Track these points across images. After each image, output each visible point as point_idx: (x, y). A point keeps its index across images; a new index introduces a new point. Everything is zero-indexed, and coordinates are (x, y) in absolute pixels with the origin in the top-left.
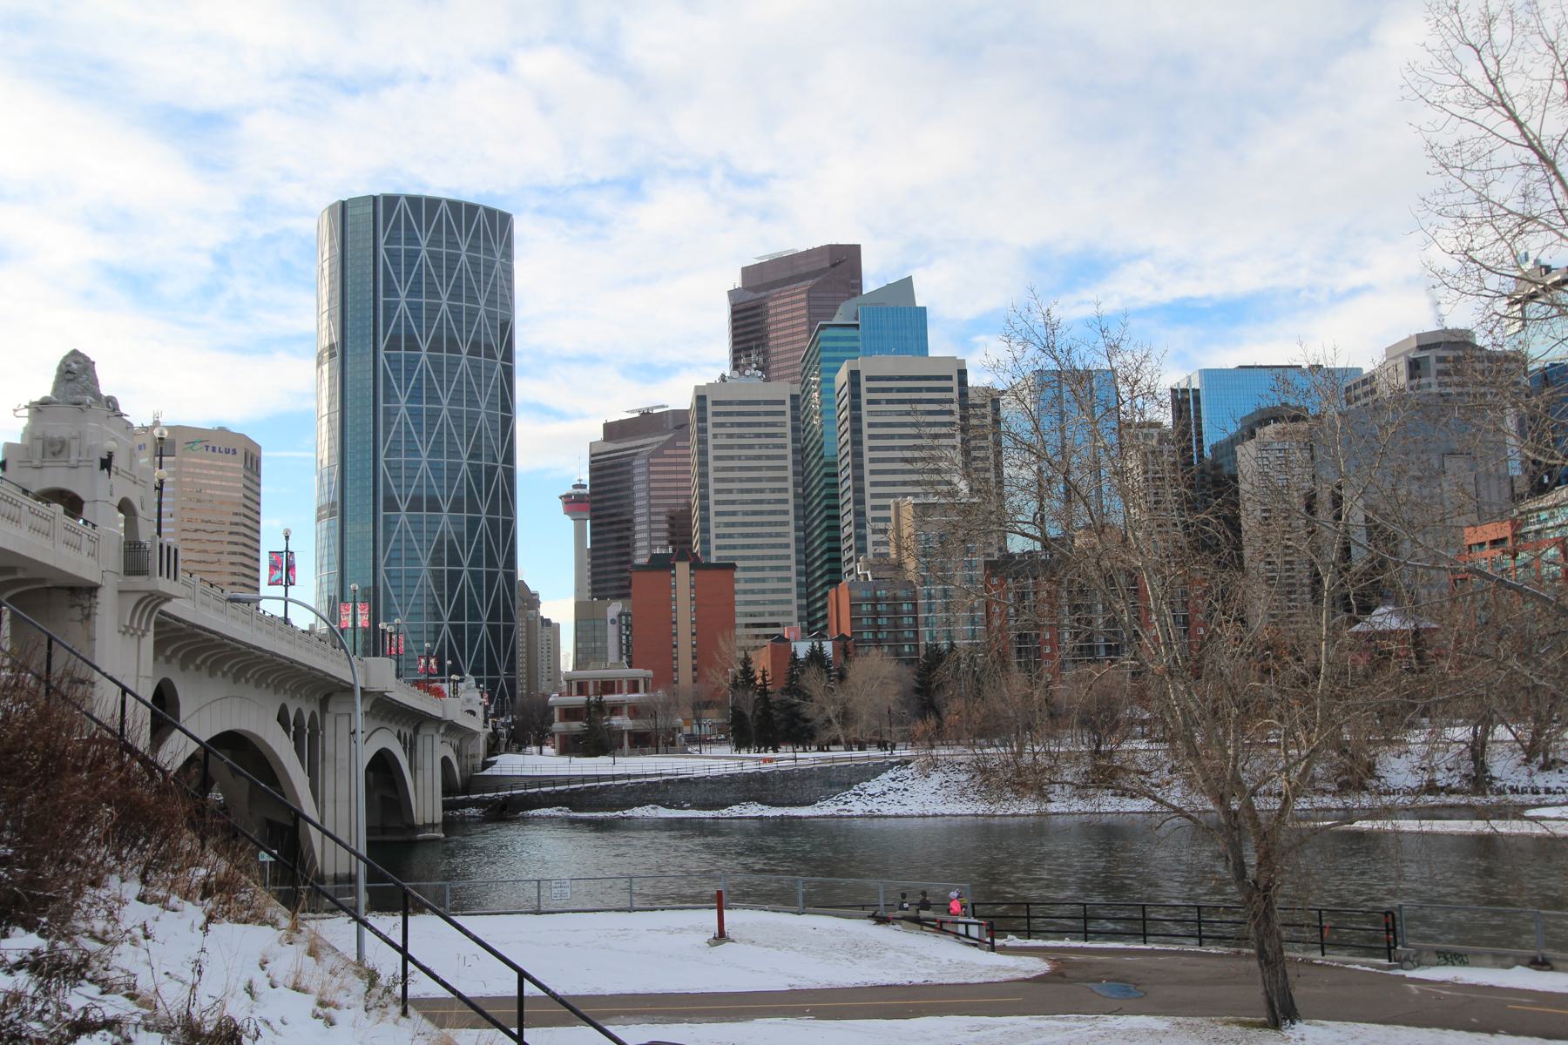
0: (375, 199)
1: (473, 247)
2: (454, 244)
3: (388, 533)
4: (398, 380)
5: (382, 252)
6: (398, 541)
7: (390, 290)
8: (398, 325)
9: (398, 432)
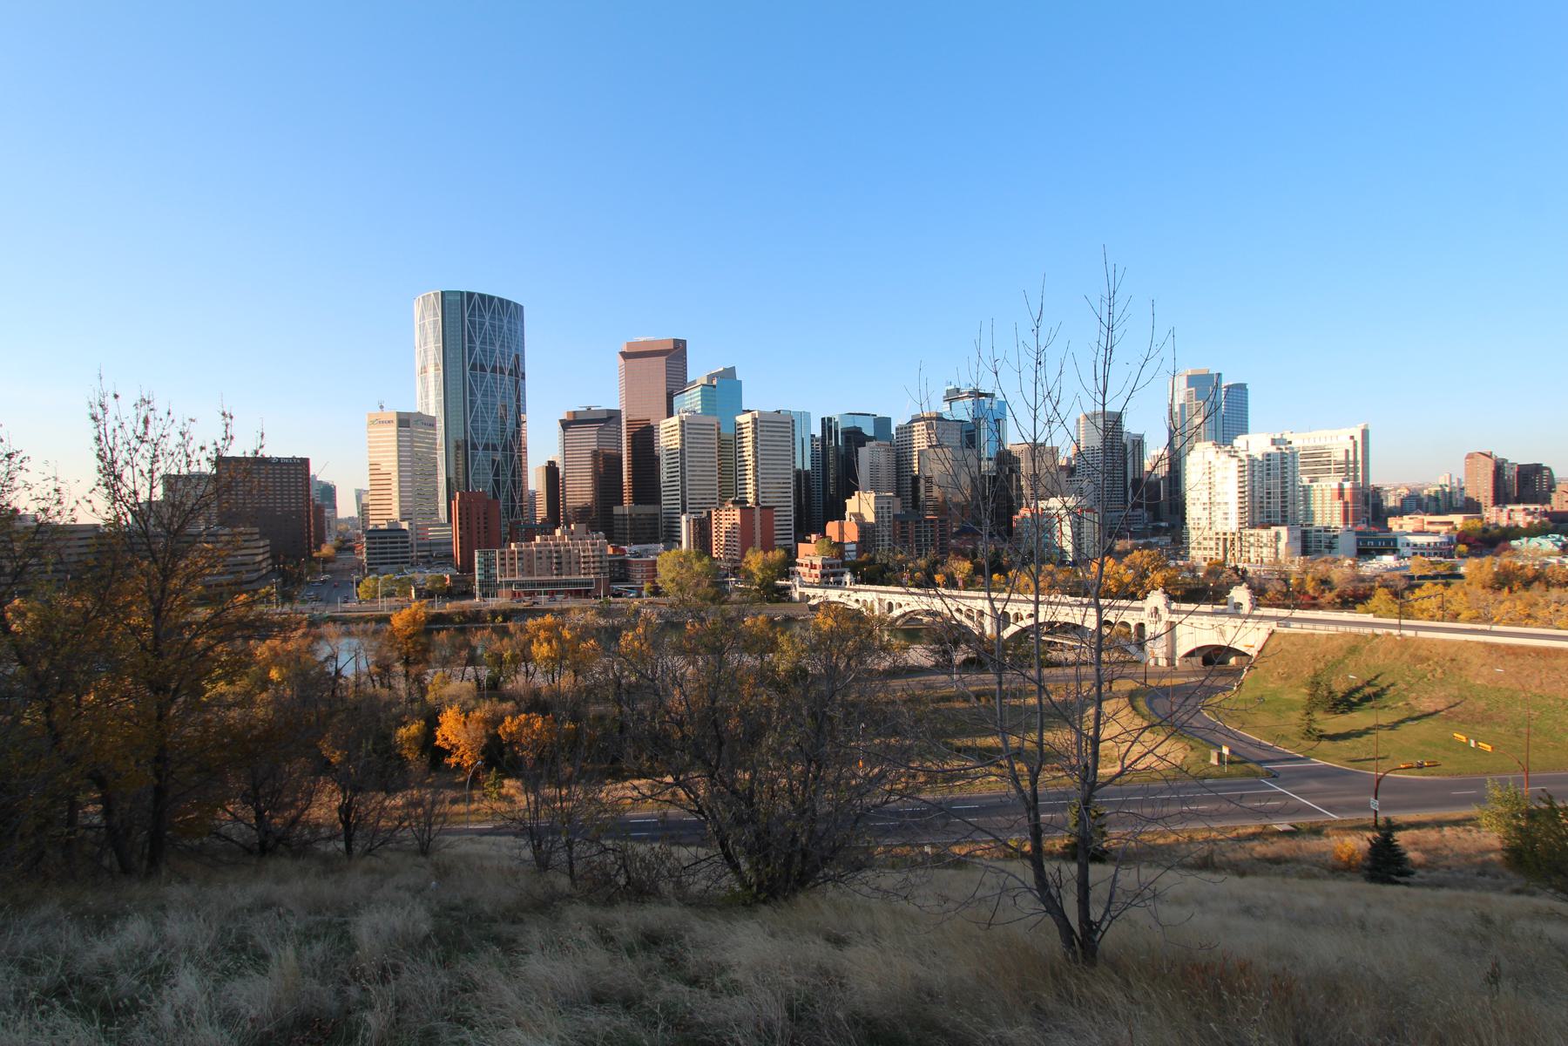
0: (462, 293)
1: (509, 322)
2: (482, 316)
3: (473, 460)
4: (476, 386)
5: (466, 321)
6: (478, 465)
7: (471, 341)
8: (476, 358)
9: (477, 412)
